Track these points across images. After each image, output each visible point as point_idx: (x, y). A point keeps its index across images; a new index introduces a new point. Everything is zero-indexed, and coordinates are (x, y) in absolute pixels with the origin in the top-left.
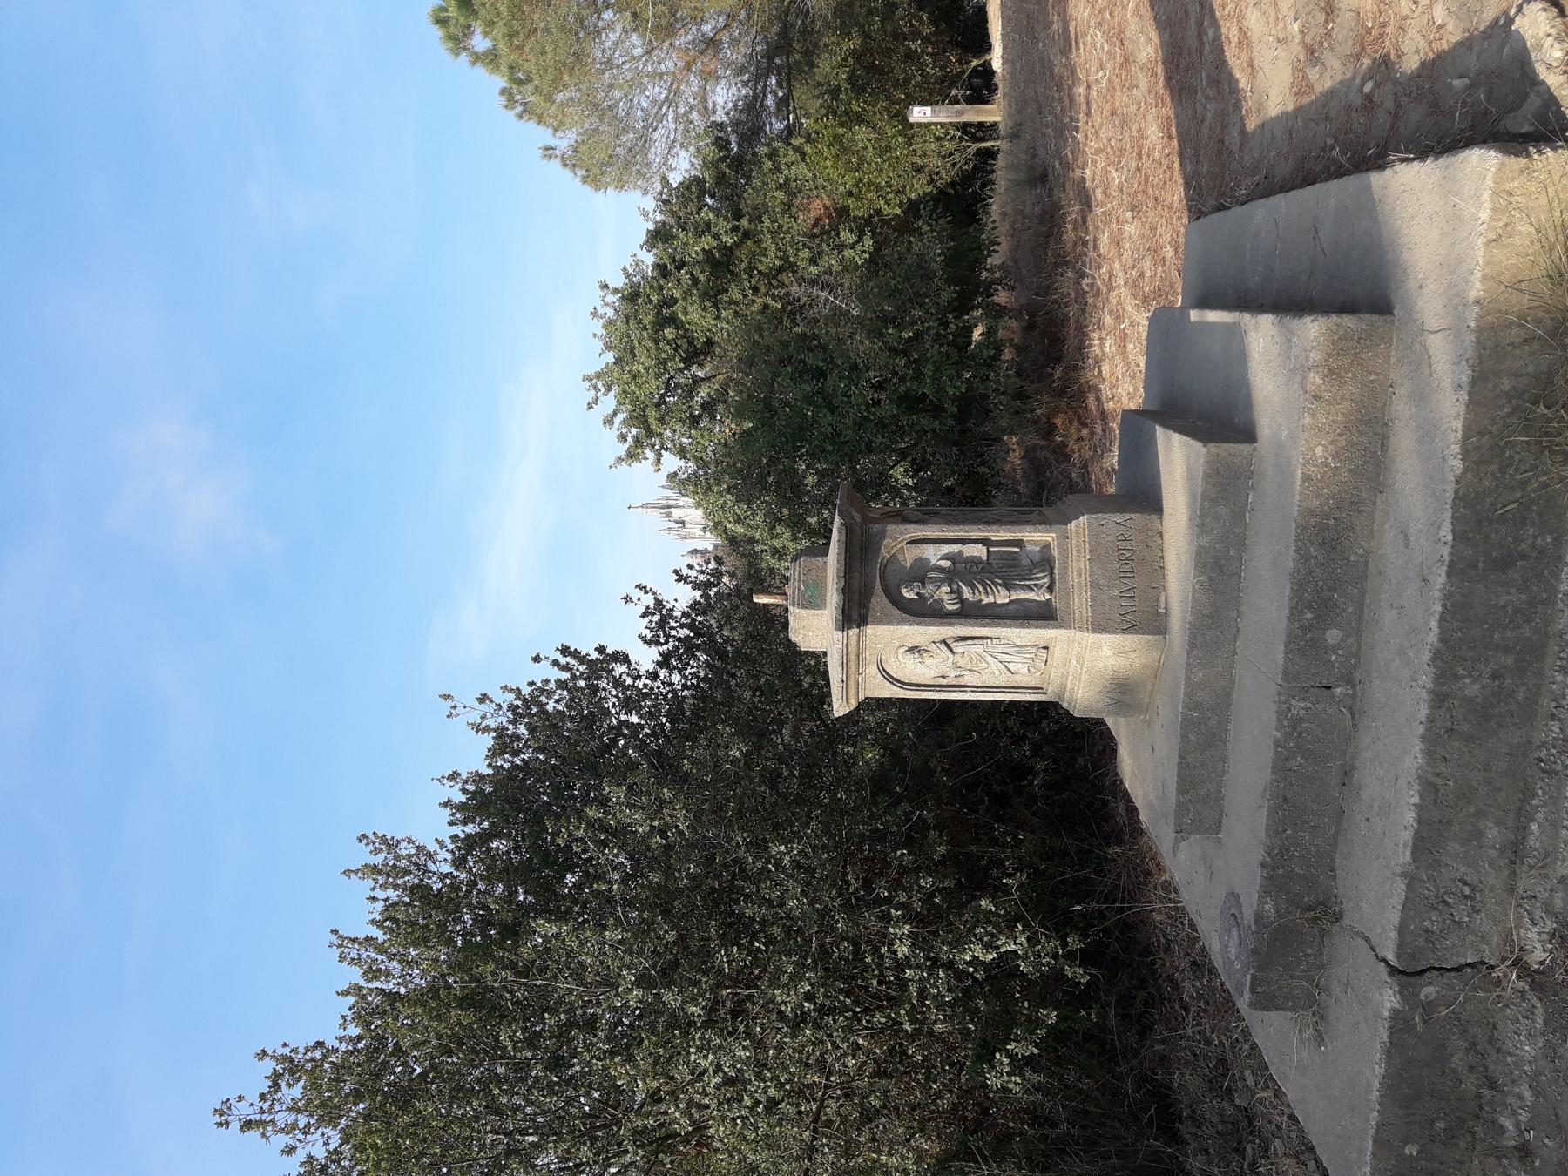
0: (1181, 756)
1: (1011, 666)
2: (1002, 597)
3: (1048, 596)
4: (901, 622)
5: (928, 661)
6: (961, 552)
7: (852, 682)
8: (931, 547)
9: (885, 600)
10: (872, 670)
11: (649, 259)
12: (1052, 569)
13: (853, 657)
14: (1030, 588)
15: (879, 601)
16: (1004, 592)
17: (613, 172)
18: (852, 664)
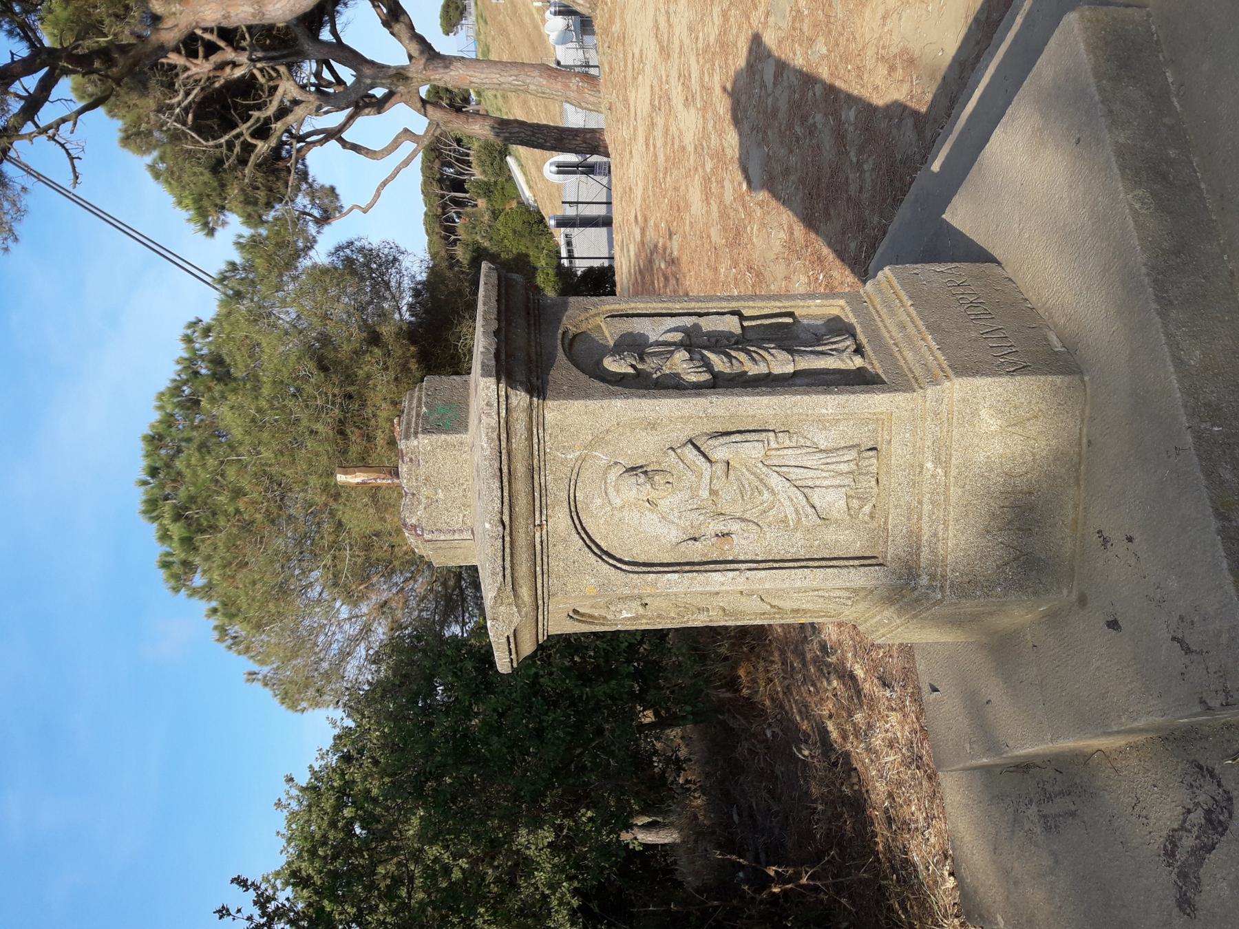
0: (1219, 515)
1: (816, 498)
2: (781, 364)
3: (858, 362)
4: (613, 395)
5: (669, 501)
6: (697, 327)
7: (522, 539)
8: (646, 321)
9: (579, 373)
10: (559, 521)
11: (333, 760)
12: (854, 336)
13: (520, 469)
14: (822, 353)
15: (562, 370)
16: (782, 355)
17: (311, 692)
18: (521, 486)
